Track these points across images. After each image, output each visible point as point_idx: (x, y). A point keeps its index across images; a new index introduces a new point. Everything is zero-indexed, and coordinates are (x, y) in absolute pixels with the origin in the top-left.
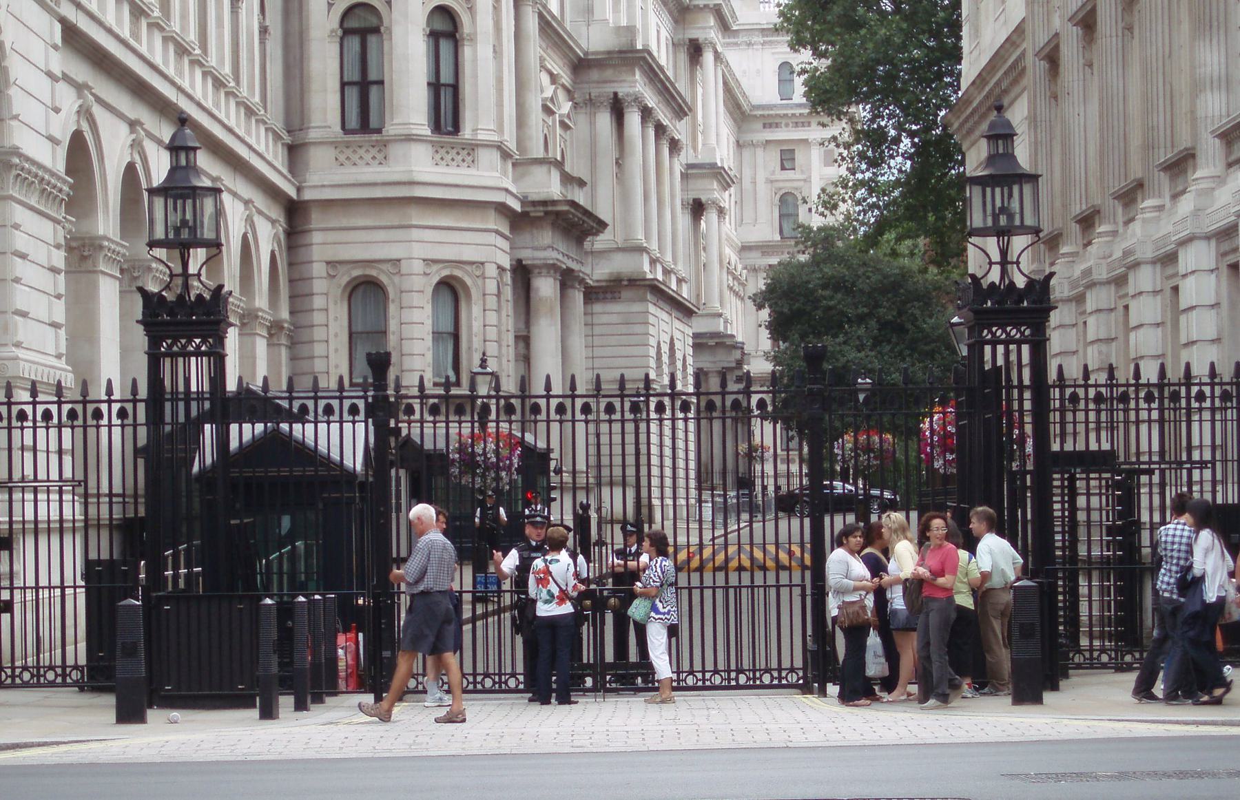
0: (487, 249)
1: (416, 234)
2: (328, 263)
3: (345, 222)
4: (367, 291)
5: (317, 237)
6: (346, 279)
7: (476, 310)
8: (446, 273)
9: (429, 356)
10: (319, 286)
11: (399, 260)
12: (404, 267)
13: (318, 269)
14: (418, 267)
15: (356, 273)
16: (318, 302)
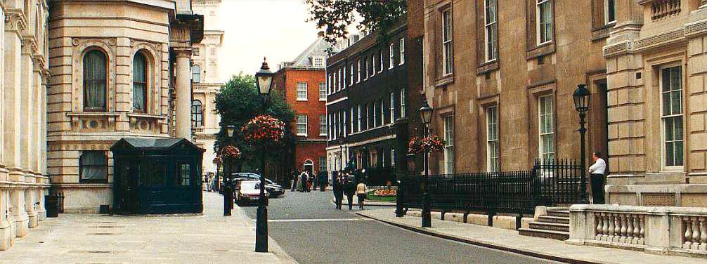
0: (160, 34)
1: (126, 23)
2: (72, 38)
3: (84, 14)
4: (96, 56)
5: (66, 23)
6: (83, 48)
7: (157, 70)
8: (141, 47)
9: (131, 95)
10: (67, 51)
11: (116, 38)
12: (119, 41)
13: (67, 41)
14: (127, 42)
15: (90, 44)
16: (66, 61)
